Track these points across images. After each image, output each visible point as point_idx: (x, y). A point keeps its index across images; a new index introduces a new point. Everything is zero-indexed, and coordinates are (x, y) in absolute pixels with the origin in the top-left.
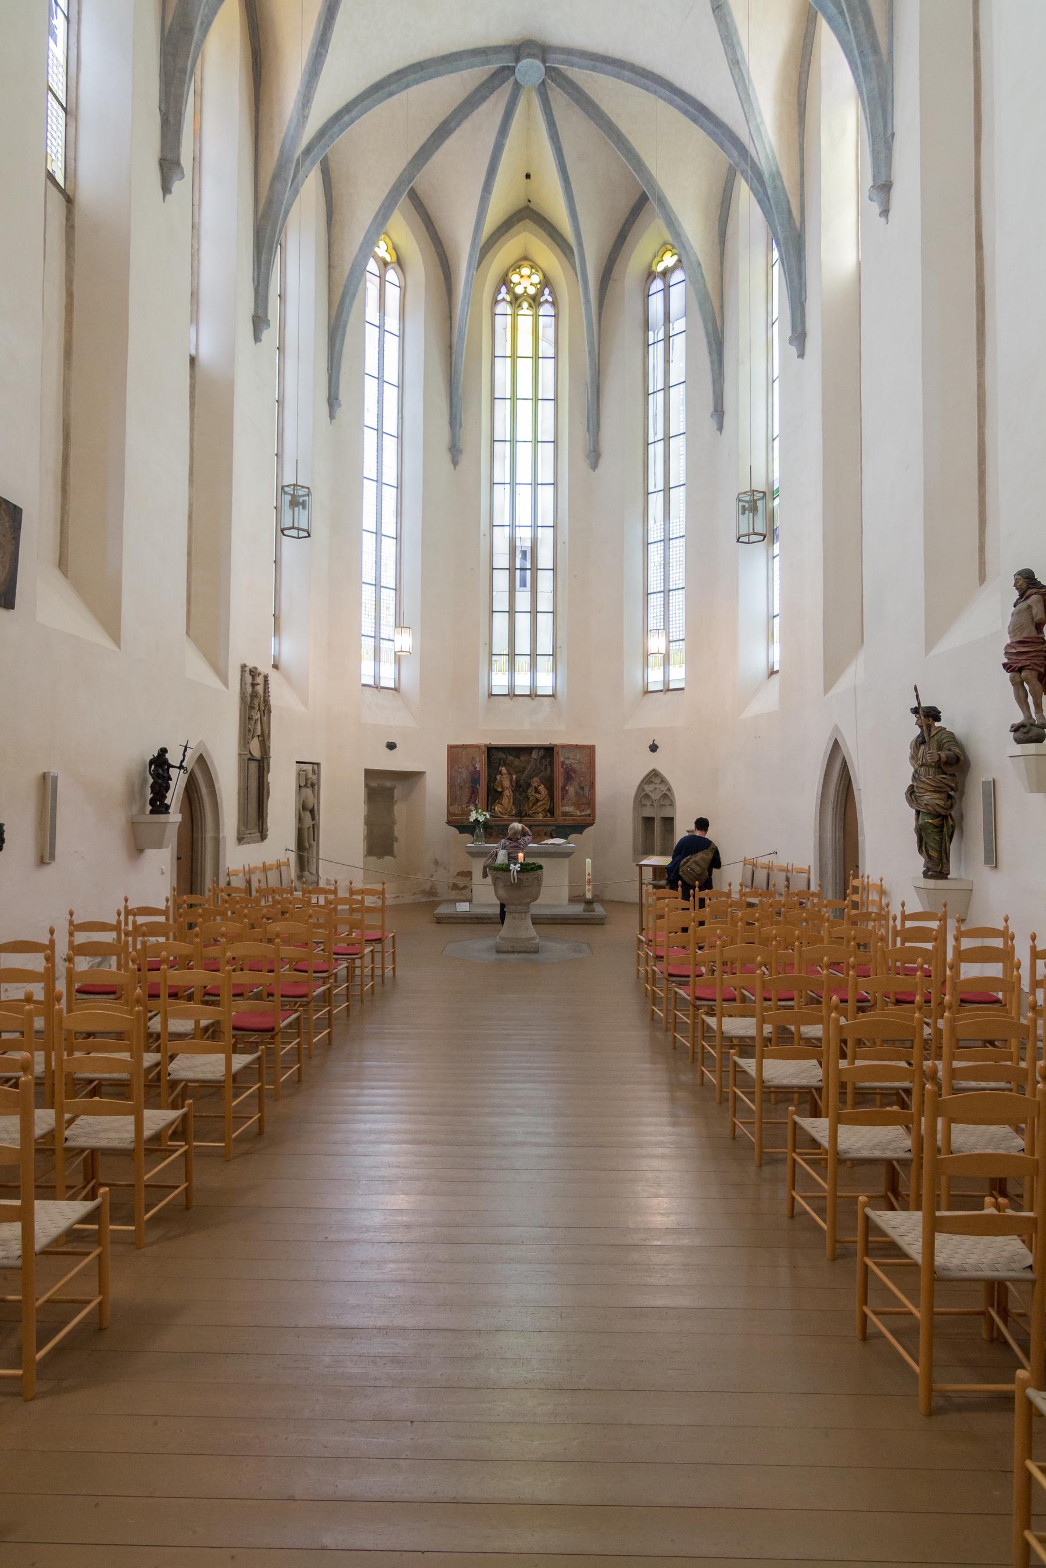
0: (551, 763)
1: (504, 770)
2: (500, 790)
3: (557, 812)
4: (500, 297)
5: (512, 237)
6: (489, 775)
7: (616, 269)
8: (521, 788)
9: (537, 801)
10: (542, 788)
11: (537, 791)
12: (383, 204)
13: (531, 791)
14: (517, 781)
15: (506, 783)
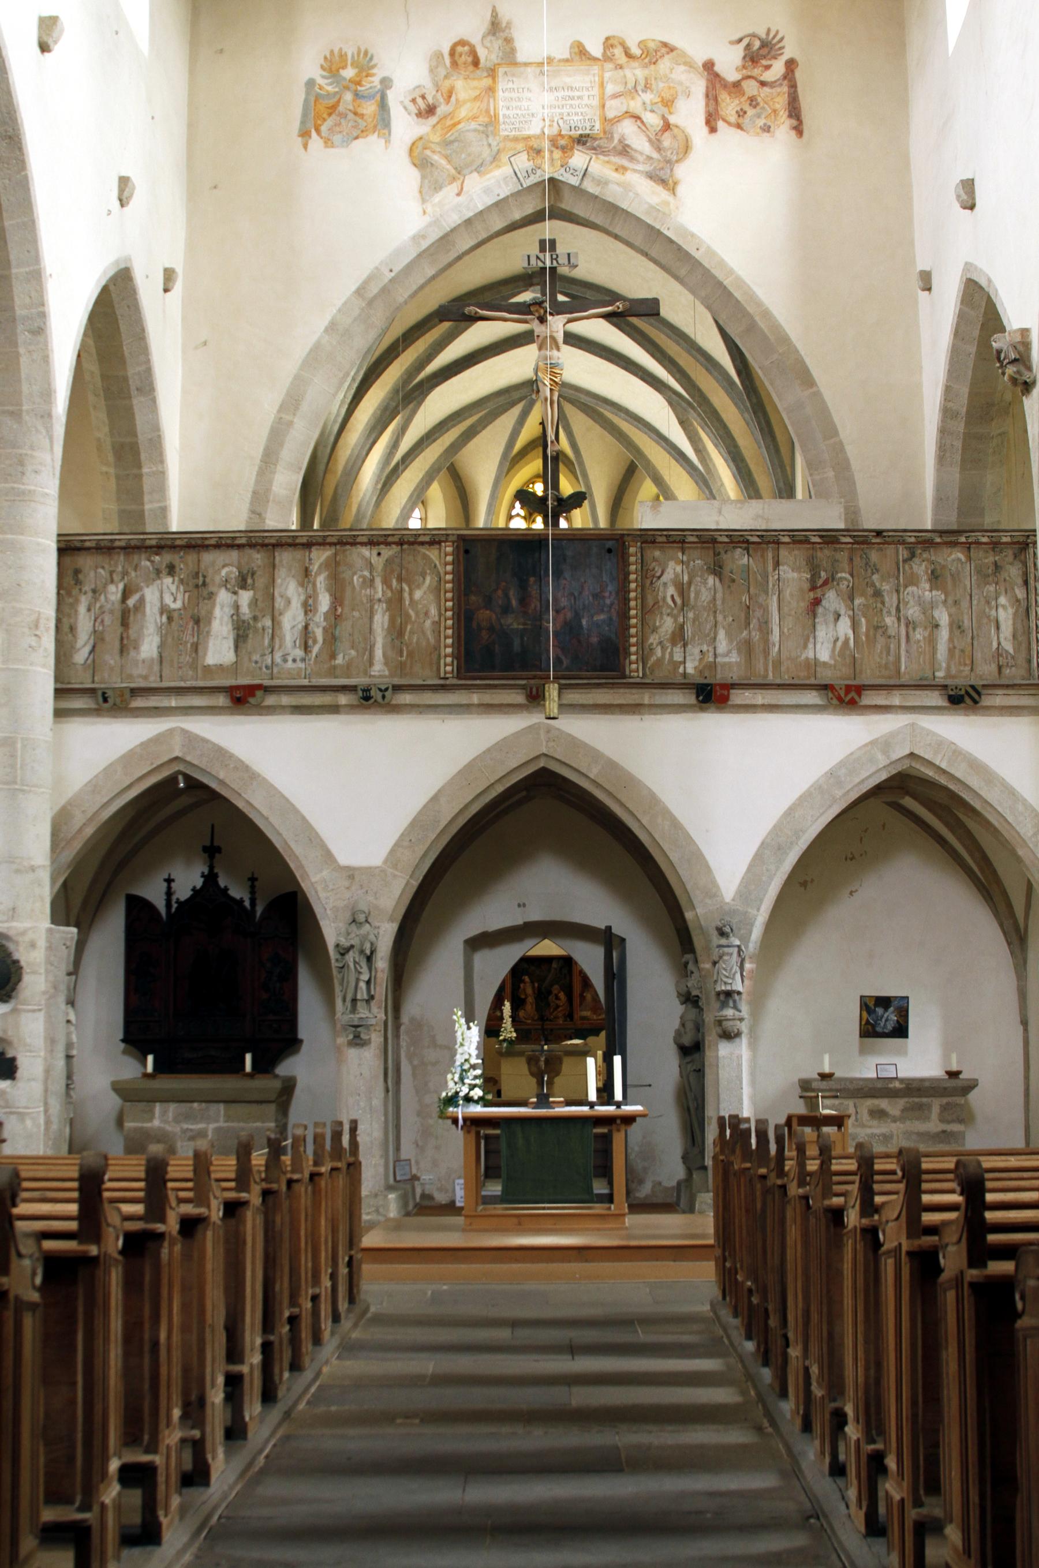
0: (570, 972)
1: (526, 978)
2: (523, 997)
3: (576, 1017)
4: (514, 513)
5: (527, 464)
6: (513, 984)
7: (626, 497)
8: (542, 996)
9: (558, 1006)
10: (562, 995)
11: (557, 998)
12: (417, 486)
13: (551, 998)
14: (539, 988)
15: (529, 991)
